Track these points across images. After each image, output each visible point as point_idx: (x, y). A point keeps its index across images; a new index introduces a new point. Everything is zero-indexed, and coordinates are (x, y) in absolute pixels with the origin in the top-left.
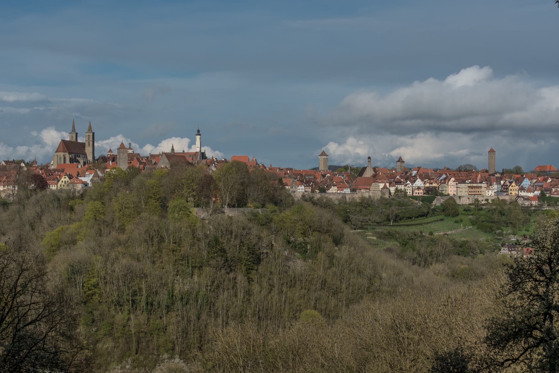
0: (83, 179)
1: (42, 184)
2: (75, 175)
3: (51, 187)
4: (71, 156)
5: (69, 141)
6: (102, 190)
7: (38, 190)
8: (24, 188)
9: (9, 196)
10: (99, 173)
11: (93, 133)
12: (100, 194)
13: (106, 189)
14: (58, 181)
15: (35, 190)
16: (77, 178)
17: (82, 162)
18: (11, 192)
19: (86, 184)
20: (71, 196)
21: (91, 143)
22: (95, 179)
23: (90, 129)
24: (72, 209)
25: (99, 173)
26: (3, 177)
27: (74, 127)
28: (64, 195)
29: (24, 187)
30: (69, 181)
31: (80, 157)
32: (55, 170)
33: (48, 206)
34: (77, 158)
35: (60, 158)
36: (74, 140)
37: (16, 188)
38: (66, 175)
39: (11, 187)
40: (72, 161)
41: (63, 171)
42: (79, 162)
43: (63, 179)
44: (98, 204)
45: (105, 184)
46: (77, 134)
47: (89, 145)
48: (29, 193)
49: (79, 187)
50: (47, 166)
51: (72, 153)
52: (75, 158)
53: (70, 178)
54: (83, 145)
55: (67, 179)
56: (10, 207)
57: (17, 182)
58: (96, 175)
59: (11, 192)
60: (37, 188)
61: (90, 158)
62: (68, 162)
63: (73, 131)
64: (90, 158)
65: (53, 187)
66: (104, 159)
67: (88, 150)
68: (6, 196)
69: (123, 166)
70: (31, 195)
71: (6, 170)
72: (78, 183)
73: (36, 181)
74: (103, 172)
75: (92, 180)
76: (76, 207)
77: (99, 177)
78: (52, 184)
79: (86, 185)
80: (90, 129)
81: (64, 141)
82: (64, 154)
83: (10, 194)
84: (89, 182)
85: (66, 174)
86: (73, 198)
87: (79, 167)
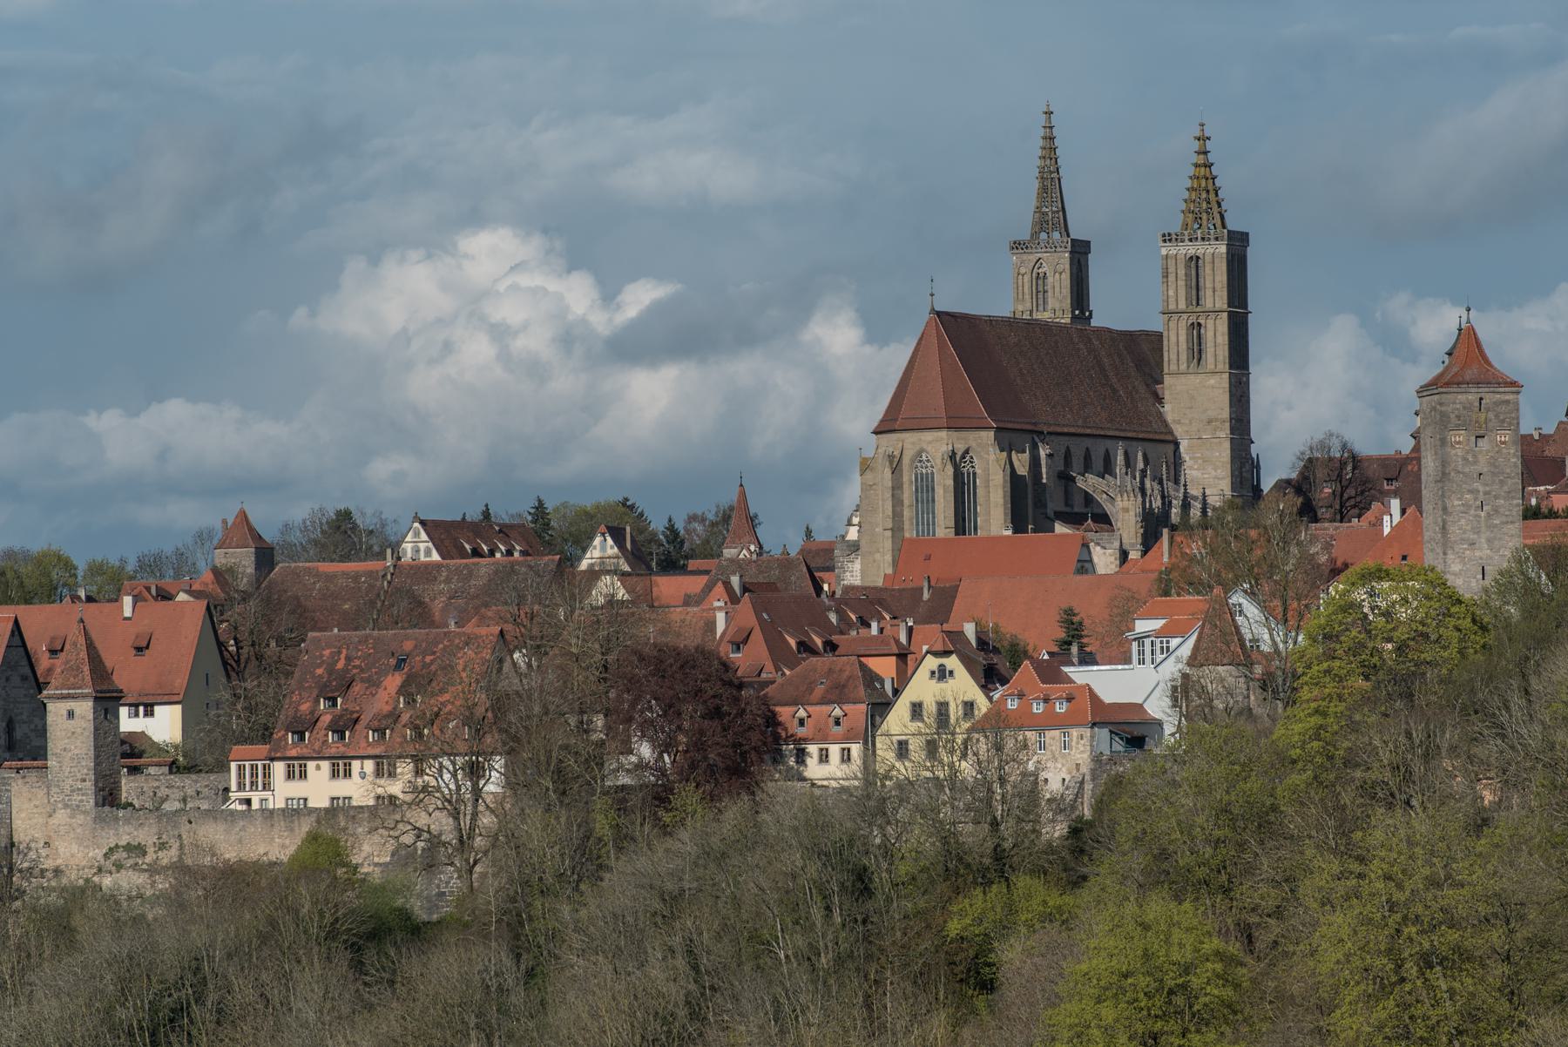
0: (1111, 683)
1: (733, 737)
2: (1042, 639)
3: (813, 769)
4: (1021, 463)
5: (1011, 323)
6: (1254, 784)
7: (688, 796)
8: (559, 778)
9: (431, 855)
10: (1251, 618)
11: (1238, 246)
12: (1213, 834)
13: (1297, 779)
14: (881, 707)
15: (661, 796)
16: (1050, 673)
17: (1126, 514)
18: (442, 824)
19: (1131, 730)
20: (1001, 853)
21: (1217, 334)
22: (1222, 677)
23: (1205, 200)
24: (975, 976)
25: (1251, 618)
26: (374, 684)
27: (1050, 183)
28: (919, 841)
29: (560, 774)
30: (983, 705)
31: (1107, 469)
32: (868, 603)
33: (761, 945)
34: (1089, 483)
35: (925, 486)
36: (1057, 308)
37: (493, 785)
38: (953, 644)
39: (446, 777)
40: (1028, 506)
41: (941, 606)
42: (1103, 519)
43: (922, 687)
44: (1188, 932)
45: (1293, 728)
46: (1080, 252)
47: (1197, 352)
48: (602, 826)
49: (1063, 763)
50: (819, 561)
51: (1036, 435)
52: (1065, 478)
53: (989, 677)
54: (1140, 356)
55: (963, 686)
56: (412, 966)
57: (497, 724)
58: (1222, 641)
59: (442, 824)
60: (688, 771)
61: (1207, 474)
62: (993, 516)
63: (1042, 224)
64: (1207, 474)
65: (829, 768)
66: (1343, 484)
67: (1191, 401)
68: (403, 857)
69: (1474, 547)
70: (622, 839)
71: (420, 614)
72: (1062, 723)
73: (671, 709)
74: (1284, 615)
75: (1182, 691)
76: (1011, 955)
77: (1244, 655)
78: (823, 737)
79: (1137, 742)
80: (1205, 200)
81: (958, 330)
82: (960, 441)
83: (435, 842)
84: (1158, 707)
85: (956, 637)
86: (1000, 866)
87: (1104, 560)
